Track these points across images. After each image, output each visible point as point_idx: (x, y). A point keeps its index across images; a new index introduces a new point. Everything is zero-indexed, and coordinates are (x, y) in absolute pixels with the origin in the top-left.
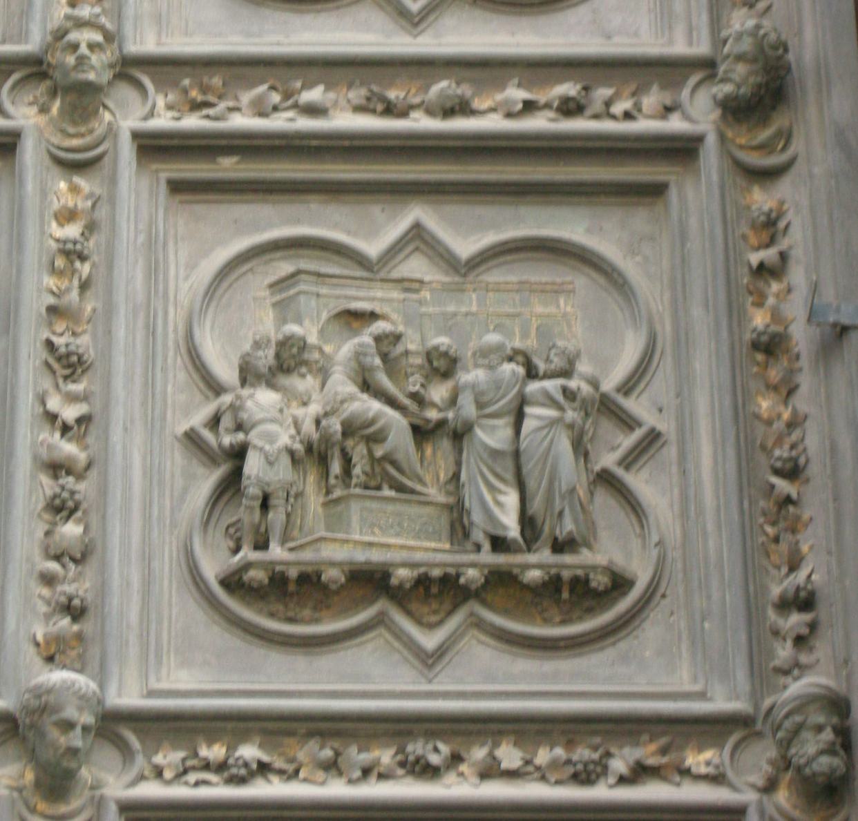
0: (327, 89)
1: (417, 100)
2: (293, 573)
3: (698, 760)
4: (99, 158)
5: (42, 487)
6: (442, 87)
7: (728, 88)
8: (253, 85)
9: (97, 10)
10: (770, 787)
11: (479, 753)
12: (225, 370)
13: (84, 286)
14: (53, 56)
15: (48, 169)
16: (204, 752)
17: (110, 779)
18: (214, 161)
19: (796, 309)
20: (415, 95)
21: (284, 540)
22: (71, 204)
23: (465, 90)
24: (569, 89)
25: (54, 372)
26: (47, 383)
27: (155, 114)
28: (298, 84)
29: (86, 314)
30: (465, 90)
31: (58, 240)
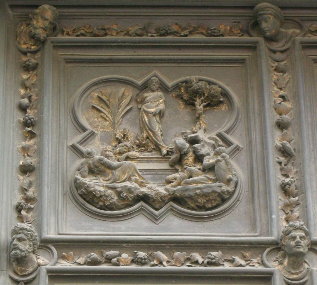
14: (284, 242)
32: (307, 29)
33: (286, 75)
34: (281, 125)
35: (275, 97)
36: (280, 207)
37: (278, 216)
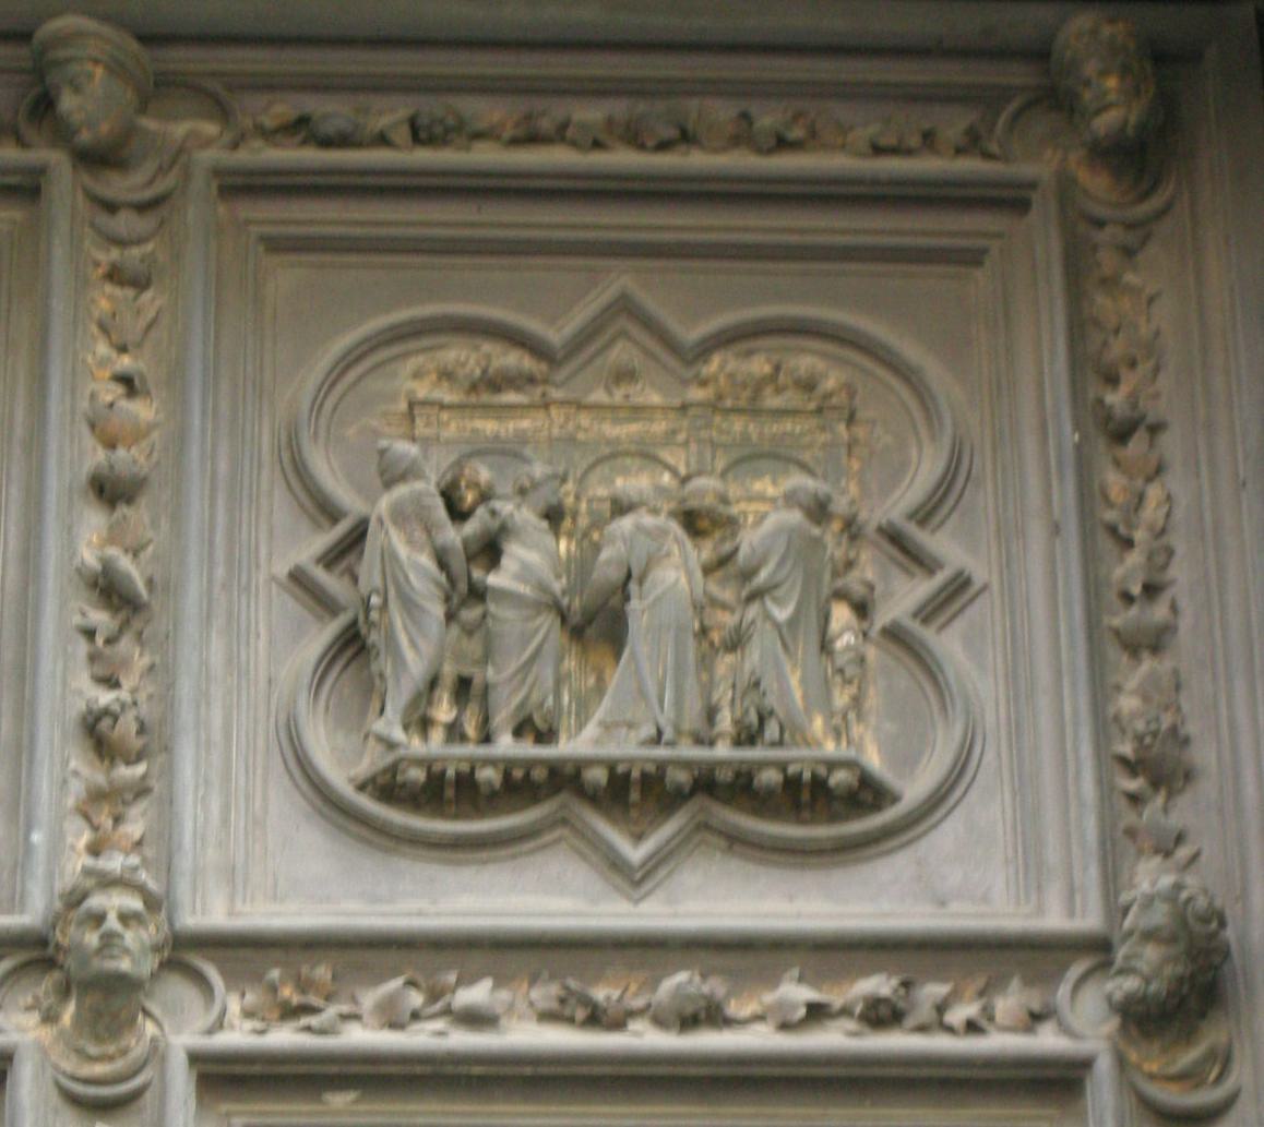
0: (497, 985)
1: (639, 1003)
4: (136, 1095)
6: (678, 982)
7: (1130, 984)
8: (381, 978)
9: (134, 860)
14: (62, 932)
15: (56, 1112)
18: (318, 1099)
20: (636, 995)
23: (716, 987)
24: (879, 984)
27: (225, 1024)
28: (452, 978)
30: (716, 987)
32: (248, 123)
33: (148, 295)
34: (107, 487)
35: (94, 378)
36: (70, 802)
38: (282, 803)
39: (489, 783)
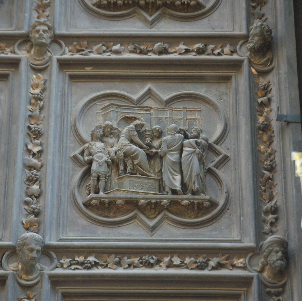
0: (121, 45)
1: (150, 49)
2: (107, 201)
3: (239, 262)
4: (46, 68)
5: (26, 173)
6: (158, 45)
7: (252, 45)
8: (96, 45)
9: (46, 19)
10: (262, 271)
11: (167, 259)
12: (86, 136)
13: (41, 109)
16: (77, 259)
17: (47, 268)
18: (84, 69)
19: (273, 116)
20: (150, 47)
21: (105, 190)
22: (37, 82)
23: (166, 46)
25: (30, 136)
26: (28, 140)
27: (65, 53)
28: (112, 44)
29: (41, 117)
30: (166, 46)
31: (32, 94)
36: (33, 8)
37: (30, 15)
38: (78, 8)
39: (120, 4)
